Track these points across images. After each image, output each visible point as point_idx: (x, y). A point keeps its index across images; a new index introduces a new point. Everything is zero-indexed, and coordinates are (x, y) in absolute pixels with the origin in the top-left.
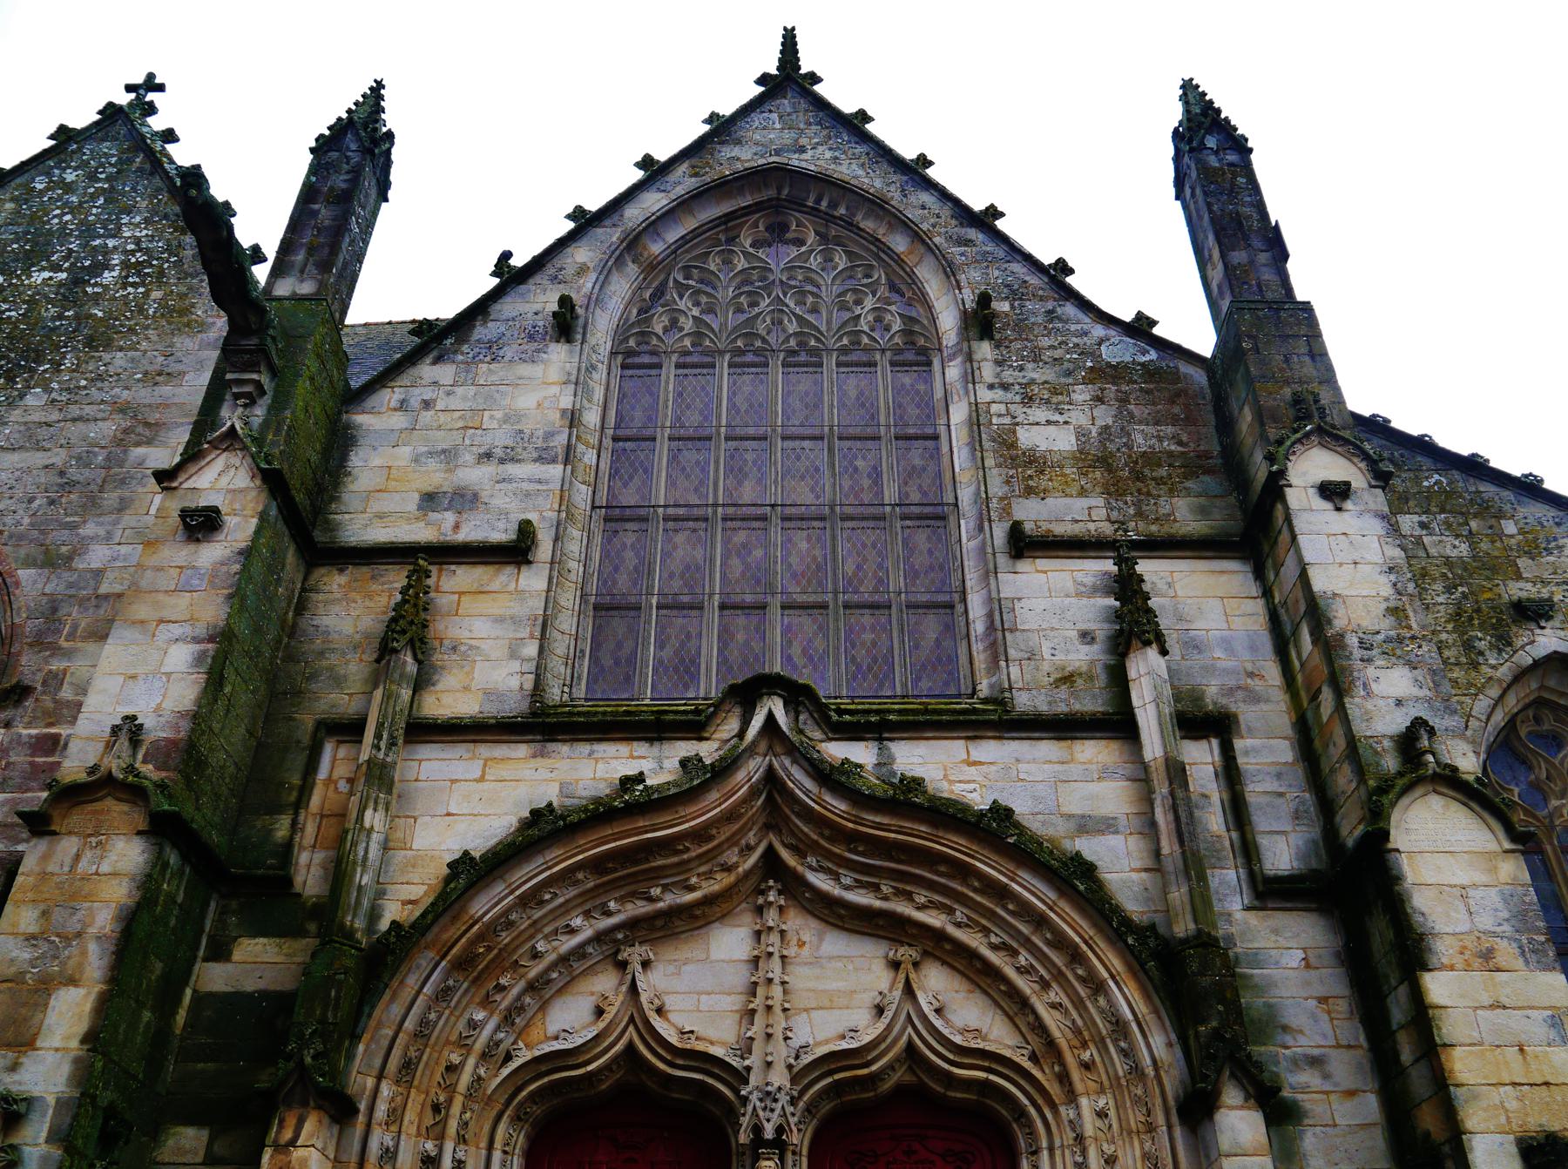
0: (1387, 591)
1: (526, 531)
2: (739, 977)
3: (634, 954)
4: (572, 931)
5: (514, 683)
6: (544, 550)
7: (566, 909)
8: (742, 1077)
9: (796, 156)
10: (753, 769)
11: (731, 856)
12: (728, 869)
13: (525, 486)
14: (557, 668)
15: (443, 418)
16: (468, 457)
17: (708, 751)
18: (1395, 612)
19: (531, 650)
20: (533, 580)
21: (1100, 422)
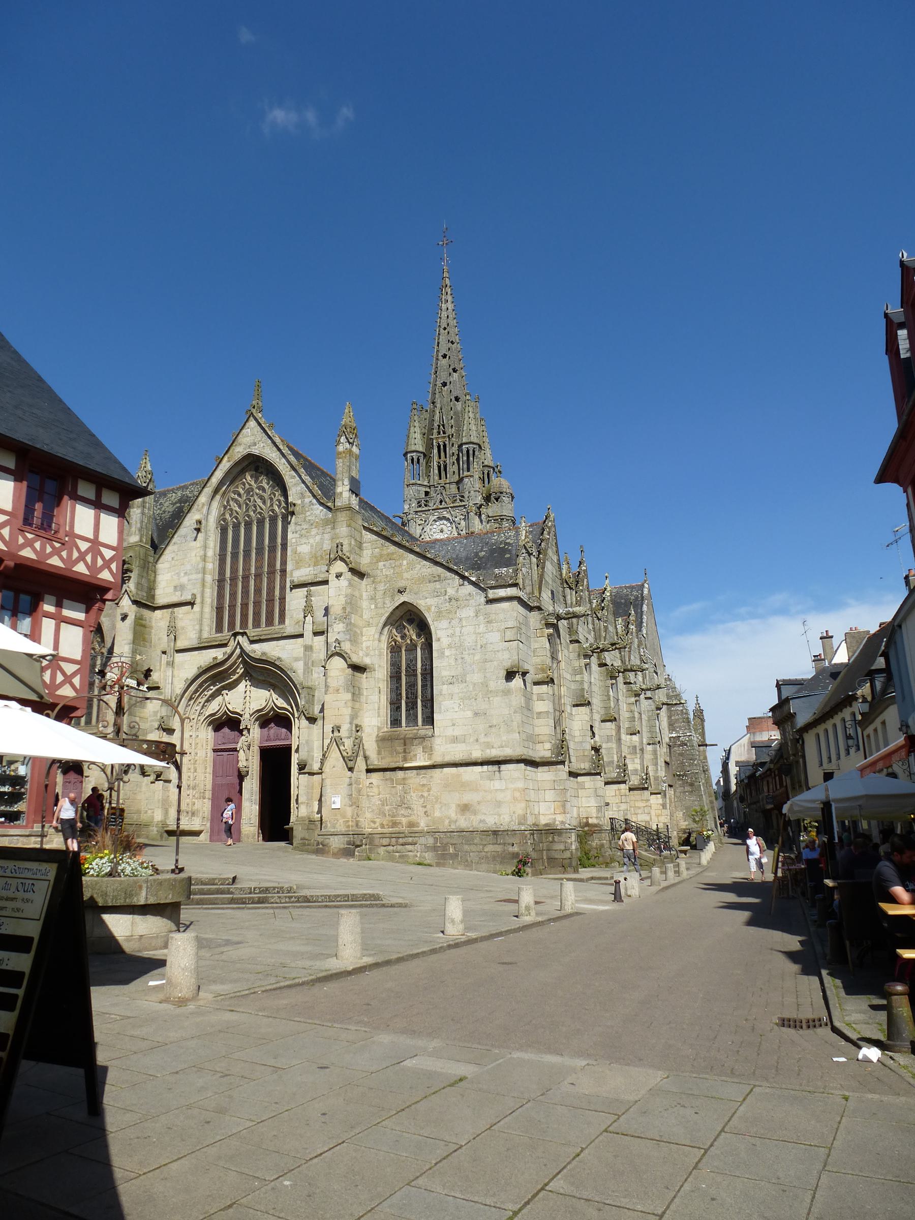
0: (343, 602)
1: (194, 595)
2: (243, 695)
3: (224, 692)
4: (211, 690)
5: (194, 636)
6: (198, 601)
7: (209, 686)
8: (241, 716)
9: (254, 447)
10: (238, 651)
11: (238, 671)
12: (238, 673)
13: (195, 581)
14: (206, 629)
15: (177, 563)
16: (182, 575)
17: (228, 650)
18: (344, 608)
19: (197, 627)
20: (197, 608)
21: (316, 541)
